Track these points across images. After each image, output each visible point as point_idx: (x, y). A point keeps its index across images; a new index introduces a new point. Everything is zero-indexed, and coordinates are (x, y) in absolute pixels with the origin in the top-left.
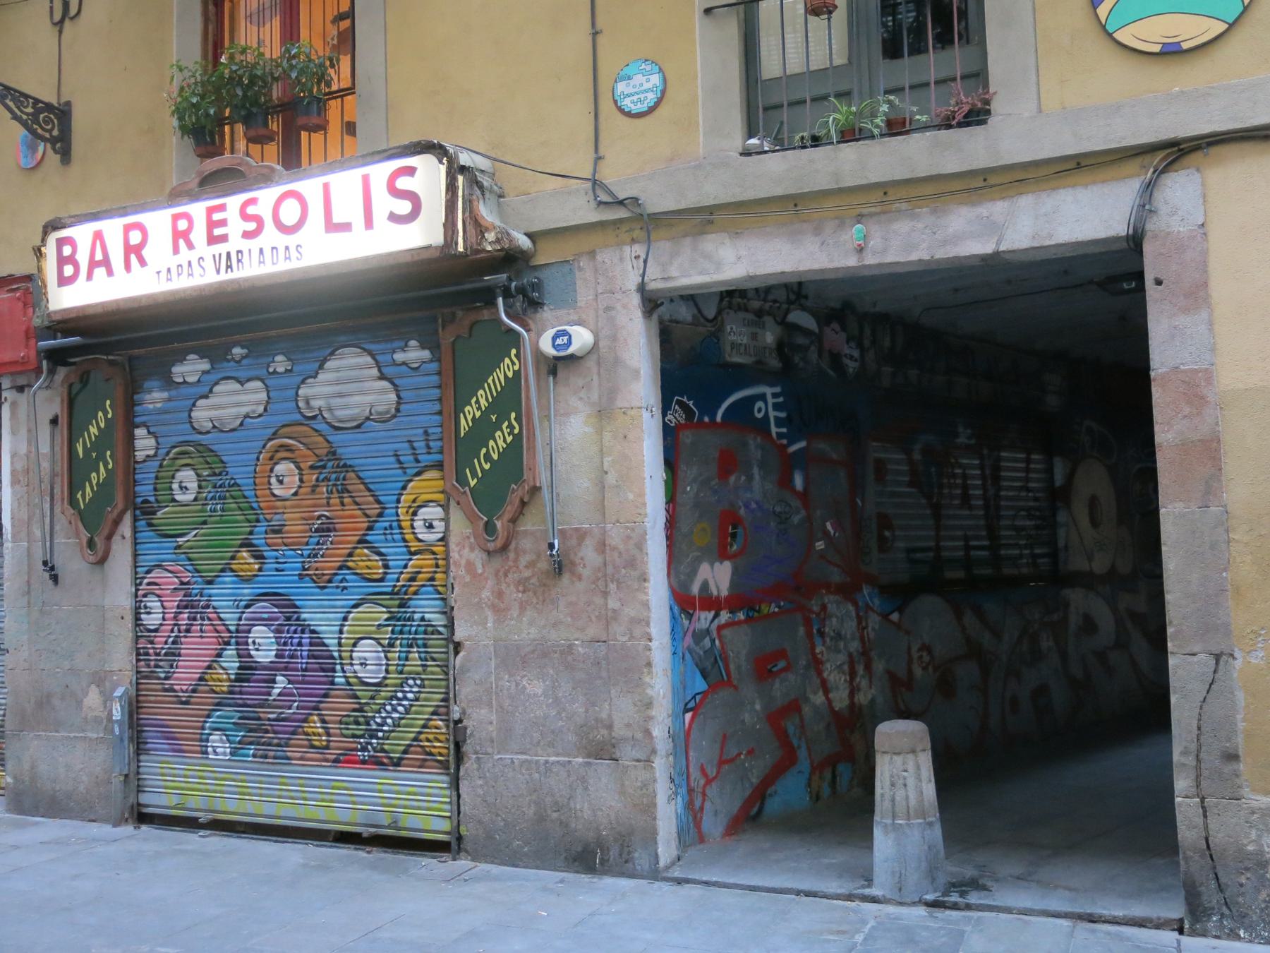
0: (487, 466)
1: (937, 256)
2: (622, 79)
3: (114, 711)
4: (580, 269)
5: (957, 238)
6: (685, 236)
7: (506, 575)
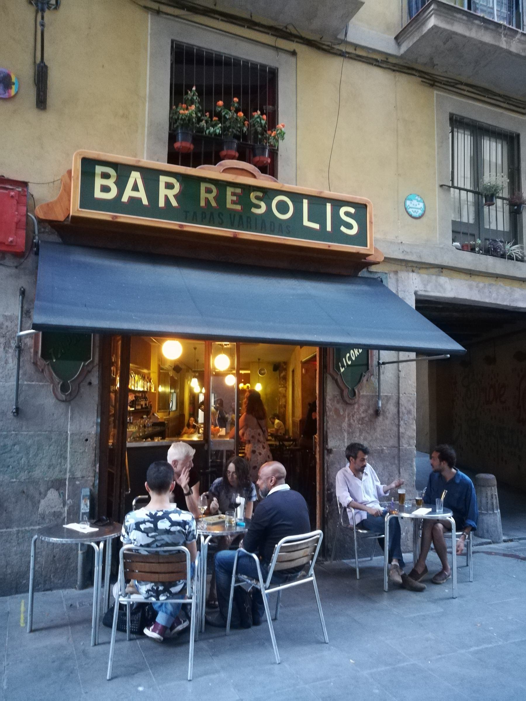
0: (350, 363)
1: (512, 305)
2: (409, 200)
3: (82, 506)
4: (390, 278)
5: (517, 300)
6: (433, 275)
7: (353, 416)
